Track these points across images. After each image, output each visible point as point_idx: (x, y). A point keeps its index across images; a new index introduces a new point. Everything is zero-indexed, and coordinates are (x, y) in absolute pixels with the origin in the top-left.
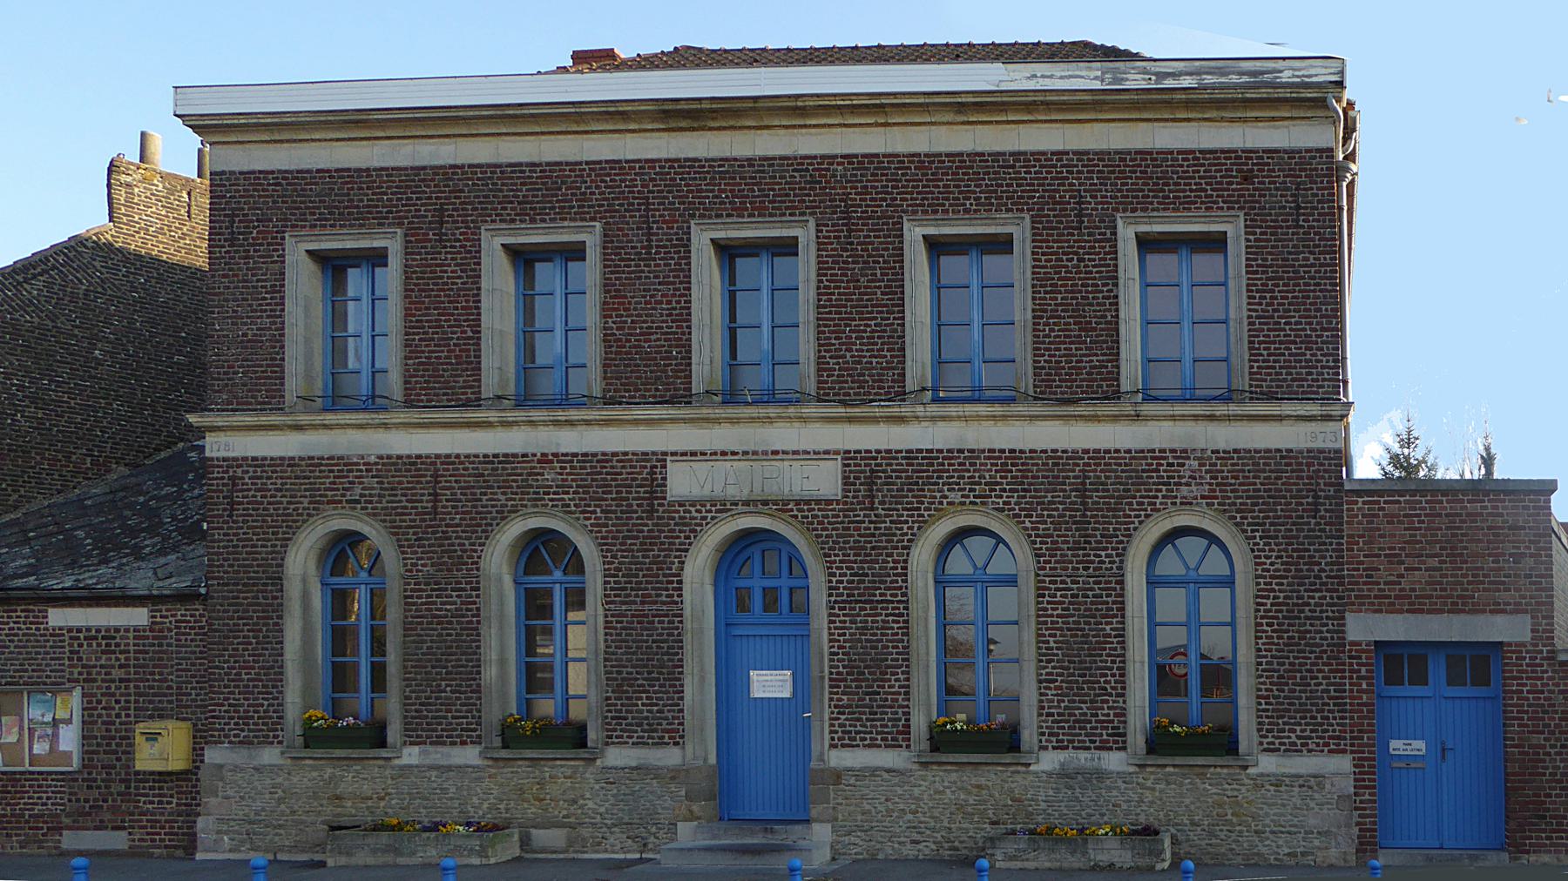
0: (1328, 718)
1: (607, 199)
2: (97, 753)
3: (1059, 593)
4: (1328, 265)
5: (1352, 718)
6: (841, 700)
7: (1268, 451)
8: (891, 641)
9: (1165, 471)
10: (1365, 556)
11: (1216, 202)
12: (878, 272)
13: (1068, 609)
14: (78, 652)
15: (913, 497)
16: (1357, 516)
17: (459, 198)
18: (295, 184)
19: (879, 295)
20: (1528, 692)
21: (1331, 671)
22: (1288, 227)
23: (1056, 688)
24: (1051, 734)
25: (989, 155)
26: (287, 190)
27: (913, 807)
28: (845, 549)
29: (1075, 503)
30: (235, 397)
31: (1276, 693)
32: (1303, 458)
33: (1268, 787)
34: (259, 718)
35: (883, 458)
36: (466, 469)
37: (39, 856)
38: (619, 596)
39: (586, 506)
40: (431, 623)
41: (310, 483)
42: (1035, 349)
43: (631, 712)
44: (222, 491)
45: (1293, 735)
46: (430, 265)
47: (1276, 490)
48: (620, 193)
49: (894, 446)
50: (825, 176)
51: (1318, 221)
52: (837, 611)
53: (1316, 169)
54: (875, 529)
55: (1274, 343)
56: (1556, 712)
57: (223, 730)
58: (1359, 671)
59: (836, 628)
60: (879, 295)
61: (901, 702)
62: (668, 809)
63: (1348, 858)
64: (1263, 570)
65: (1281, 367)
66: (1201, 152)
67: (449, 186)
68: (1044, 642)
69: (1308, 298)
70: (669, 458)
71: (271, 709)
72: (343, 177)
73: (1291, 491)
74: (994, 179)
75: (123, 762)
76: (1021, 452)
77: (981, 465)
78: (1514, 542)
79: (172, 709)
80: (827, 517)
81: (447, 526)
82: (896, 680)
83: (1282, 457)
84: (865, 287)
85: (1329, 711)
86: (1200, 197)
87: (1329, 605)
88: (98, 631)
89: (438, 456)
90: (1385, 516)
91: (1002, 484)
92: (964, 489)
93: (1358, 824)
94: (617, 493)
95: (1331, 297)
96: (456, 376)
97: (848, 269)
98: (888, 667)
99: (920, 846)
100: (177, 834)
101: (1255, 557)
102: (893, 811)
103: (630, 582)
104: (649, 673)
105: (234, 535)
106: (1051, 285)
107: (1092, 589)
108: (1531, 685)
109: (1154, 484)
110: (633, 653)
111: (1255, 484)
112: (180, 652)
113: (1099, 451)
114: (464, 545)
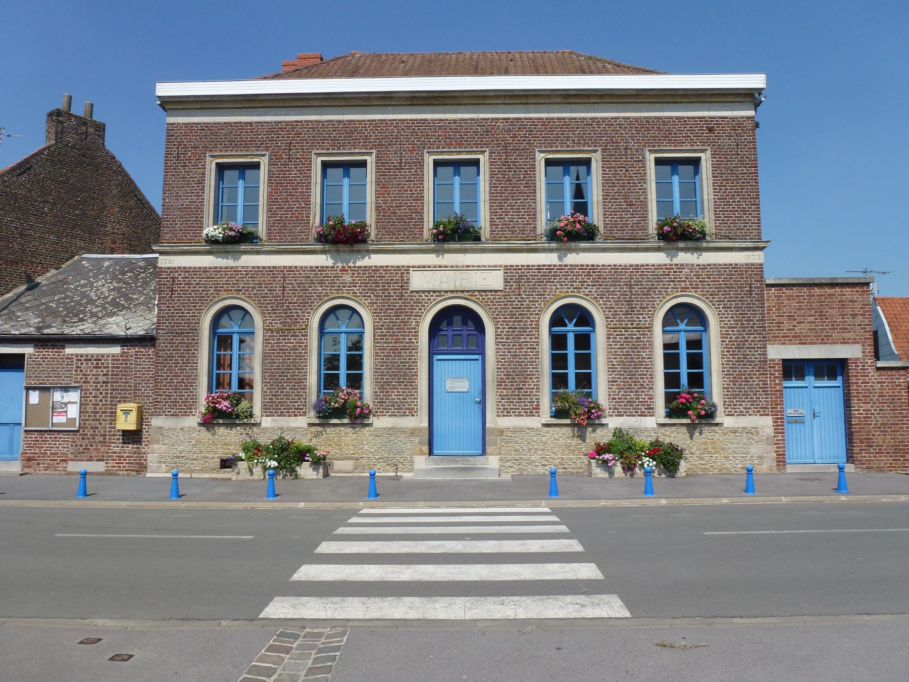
0: (759, 398)
1: (379, 139)
2: (88, 420)
3: (618, 337)
4: (753, 173)
5: (771, 398)
6: (502, 392)
7: (725, 265)
8: (529, 362)
9: (673, 275)
10: (776, 316)
11: (696, 143)
12: (522, 176)
13: (623, 345)
14: (80, 367)
15: (541, 289)
16: (771, 297)
17: (300, 137)
18: (212, 130)
19: (522, 188)
20: (862, 383)
21: (760, 375)
22: (733, 155)
23: (617, 385)
24: (615, 409)
25: (579, 119)
26: (207, 133)
27: (542, 447)
28: (505, 315)
29: (626, 291)
30: (176, 237)
31: (732, 386)
32: (743, 268)
33: (730, 434)
34: (182, 402)
35: (525, 269)
36: (301, 274)
37: (55, 474)
38: (383, 339)
39: (365, 293)
40: (279, 353)
41: (215, 281)
42: (604, 215)
43: (388, 399)
44: (166, 285)
45: (741, 407)
46: (283, 171)
47: (730, 284)
48: (385, 136)
49: (531, 263)
50: (494, 129)
51: (748, 151)
52: (500, 347)
53: (746, 127)
54: (521, 305)
55: (727, 211)
56: (876, 393)
57: (162, 408)
58: (775, 374)
59: (500, 355)
60: (522, 188)
61: (534, 393)
62: (409, 449)
63: (773, 468)
64: (724, 324)
65: (730, 223)
66: (687, 118)
67: (294, 131)
68: (610, 362)
69: (744, 189)
70: (411, 269)
71: (189, 397)
72: (237, 126)
73: (738, 284)
74: (582, 131)
75: (103, 425)
76: (598, 266)
77: (577, 272)
78: (852, 308)
79: (131, 398)
80: (495, 299)
81: (290, 303)
82: (532, 382)
83: (733, 268)
84: (515, 184)
85: (760, 395)
86: (688, 140)
87: (758, 341)
88: (92, 356)
89: (285, 267)
90: (786, 296)
91: (587, 282)
92: (568, 285)
93: (776, 451)
94: (383, 286)
95: (755, 189)
96: (295, 226)
97: (506, 175)
98: (528, 375)
99: (546, 468)
100: (133, 463)
101: (720, 318)
102: (531, 449)
103: (389, 332)
104: (398, 379)
105: (172, 307)
106: (612, 183)
107: (635, 335)
108: (863, 380)
109: (667, 281)
110: (389, 369)
111: (719, 281)
112: (137, 368)
113: (638, 265)
114: (298, 313)
